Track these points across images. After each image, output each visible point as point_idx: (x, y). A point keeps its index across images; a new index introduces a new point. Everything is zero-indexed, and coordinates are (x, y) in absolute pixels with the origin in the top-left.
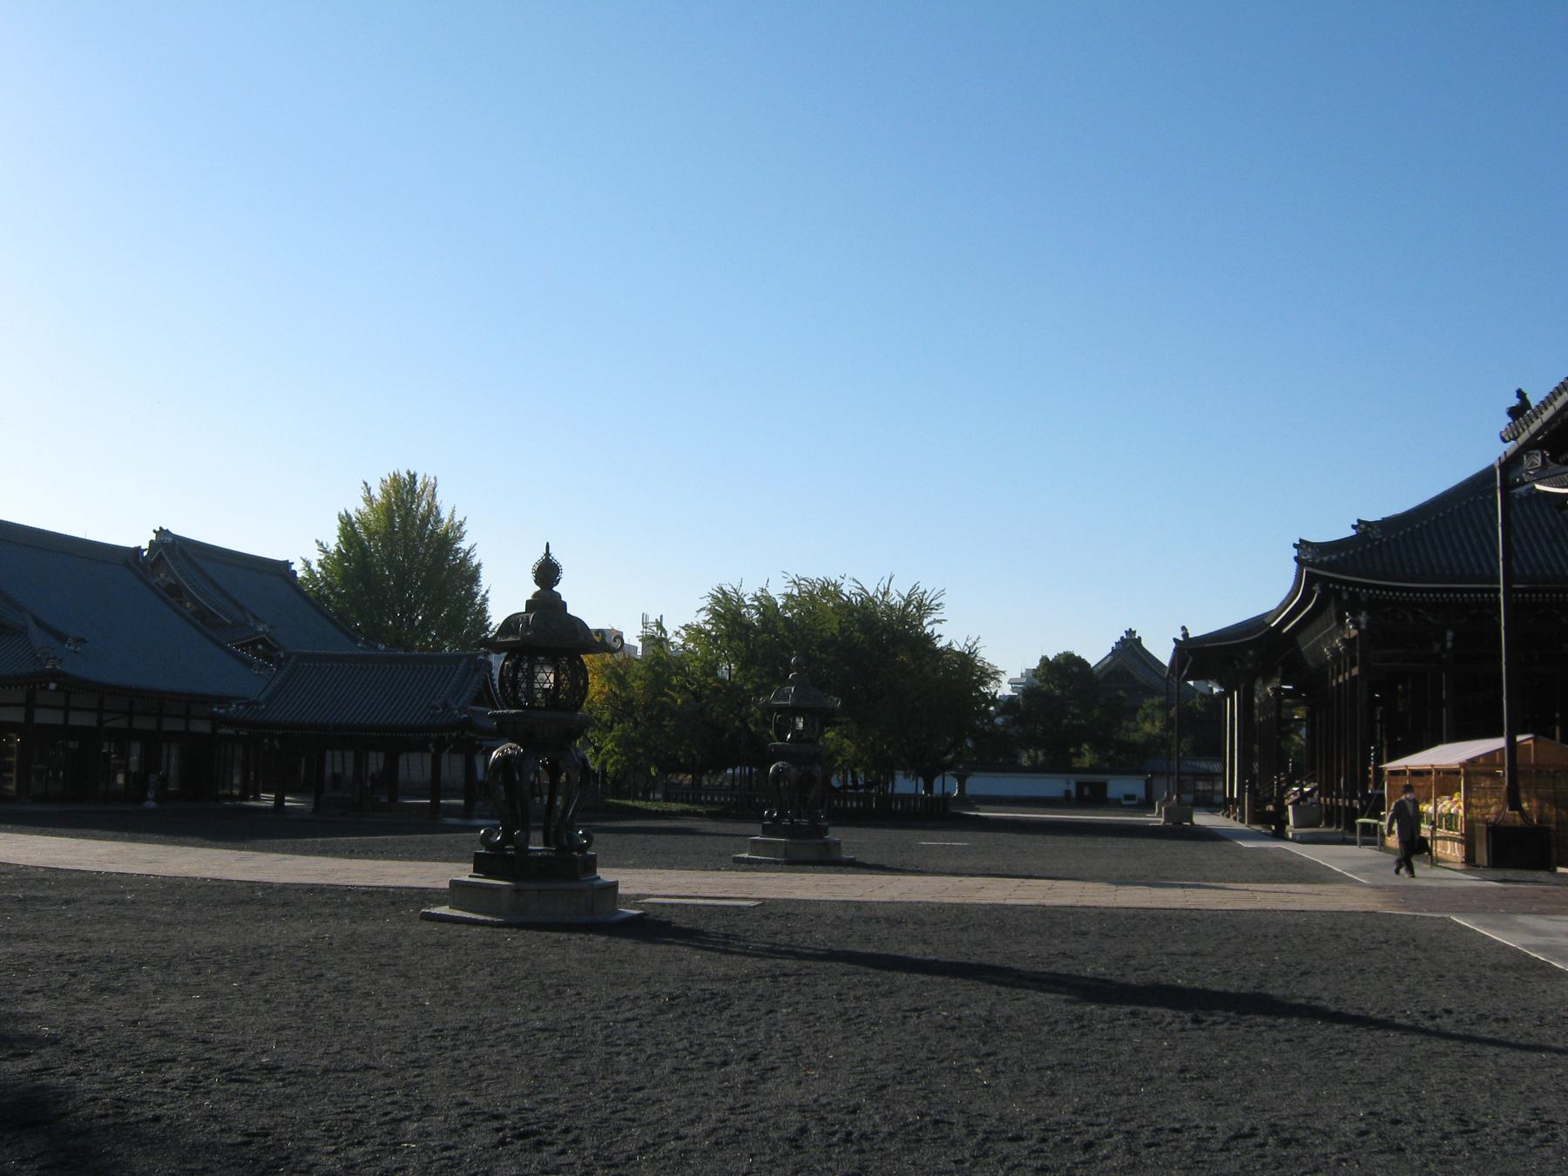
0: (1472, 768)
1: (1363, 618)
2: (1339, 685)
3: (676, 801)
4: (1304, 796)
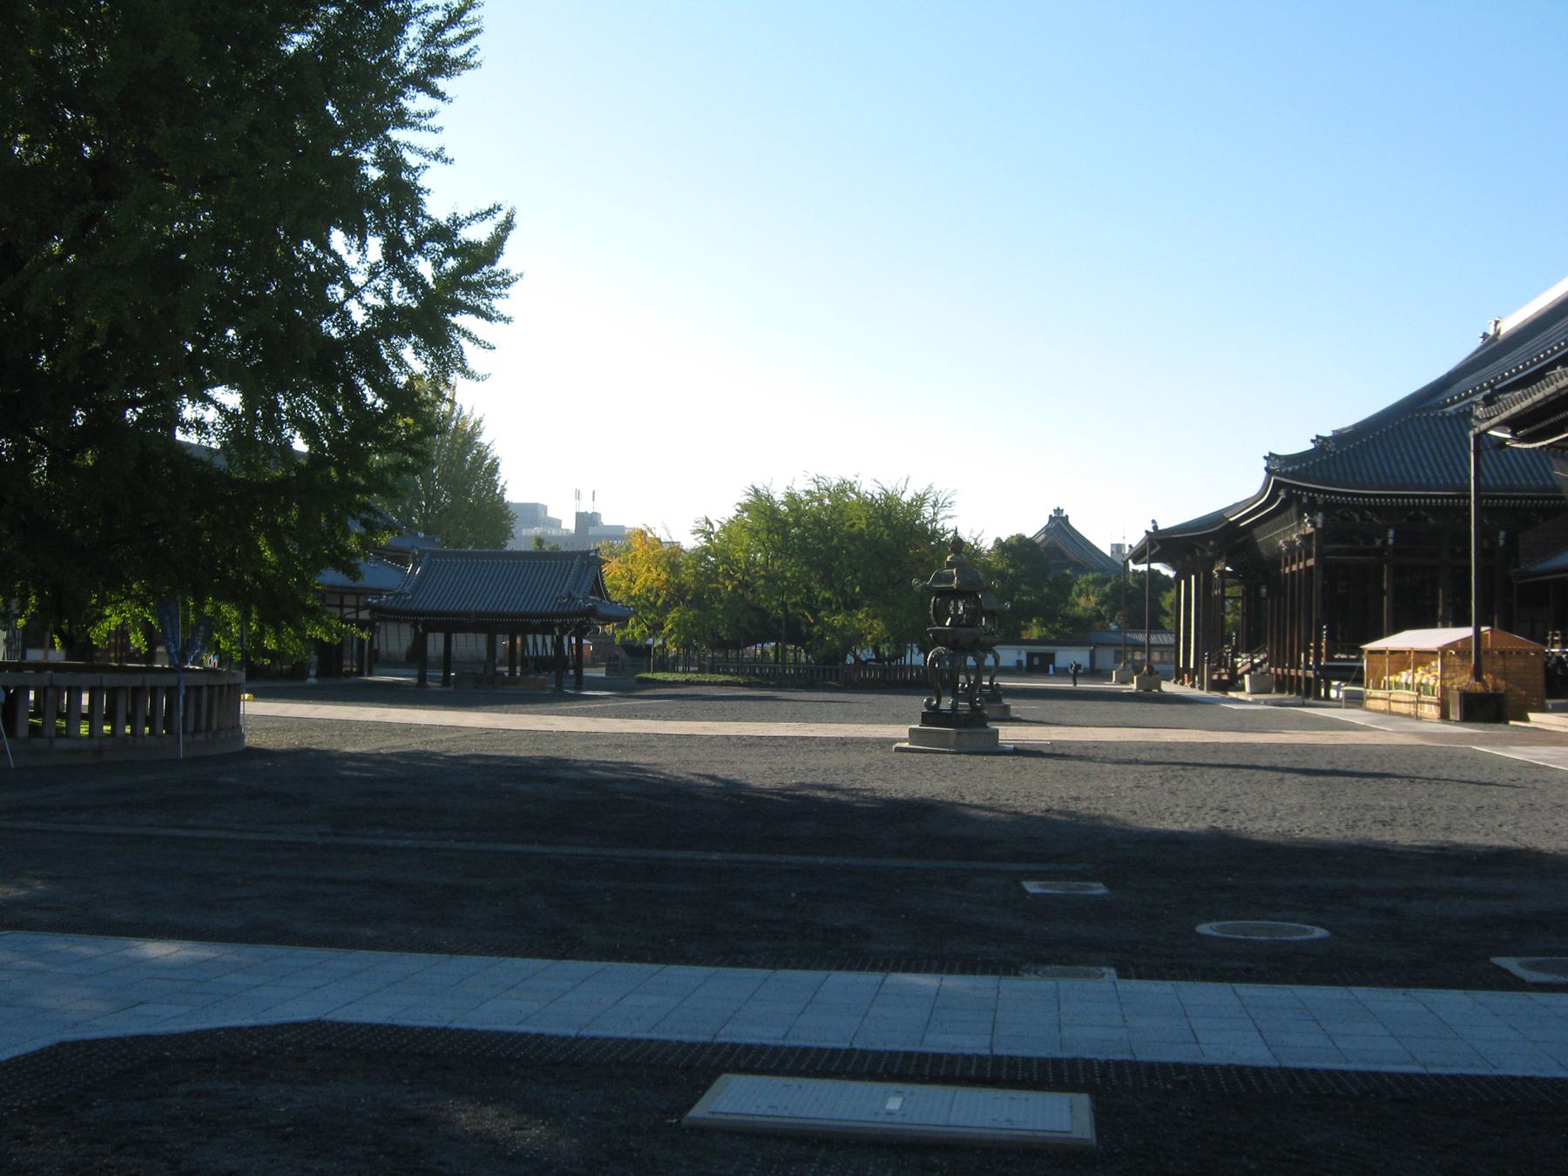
0: (1443, 651)
1: (1319, 519)
2: (1293, 573)
3: (725, 673)
4: (1254, 667)
